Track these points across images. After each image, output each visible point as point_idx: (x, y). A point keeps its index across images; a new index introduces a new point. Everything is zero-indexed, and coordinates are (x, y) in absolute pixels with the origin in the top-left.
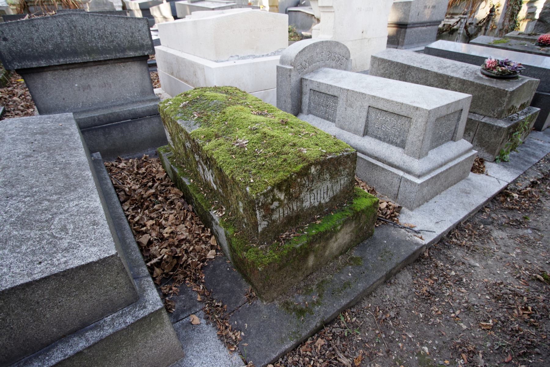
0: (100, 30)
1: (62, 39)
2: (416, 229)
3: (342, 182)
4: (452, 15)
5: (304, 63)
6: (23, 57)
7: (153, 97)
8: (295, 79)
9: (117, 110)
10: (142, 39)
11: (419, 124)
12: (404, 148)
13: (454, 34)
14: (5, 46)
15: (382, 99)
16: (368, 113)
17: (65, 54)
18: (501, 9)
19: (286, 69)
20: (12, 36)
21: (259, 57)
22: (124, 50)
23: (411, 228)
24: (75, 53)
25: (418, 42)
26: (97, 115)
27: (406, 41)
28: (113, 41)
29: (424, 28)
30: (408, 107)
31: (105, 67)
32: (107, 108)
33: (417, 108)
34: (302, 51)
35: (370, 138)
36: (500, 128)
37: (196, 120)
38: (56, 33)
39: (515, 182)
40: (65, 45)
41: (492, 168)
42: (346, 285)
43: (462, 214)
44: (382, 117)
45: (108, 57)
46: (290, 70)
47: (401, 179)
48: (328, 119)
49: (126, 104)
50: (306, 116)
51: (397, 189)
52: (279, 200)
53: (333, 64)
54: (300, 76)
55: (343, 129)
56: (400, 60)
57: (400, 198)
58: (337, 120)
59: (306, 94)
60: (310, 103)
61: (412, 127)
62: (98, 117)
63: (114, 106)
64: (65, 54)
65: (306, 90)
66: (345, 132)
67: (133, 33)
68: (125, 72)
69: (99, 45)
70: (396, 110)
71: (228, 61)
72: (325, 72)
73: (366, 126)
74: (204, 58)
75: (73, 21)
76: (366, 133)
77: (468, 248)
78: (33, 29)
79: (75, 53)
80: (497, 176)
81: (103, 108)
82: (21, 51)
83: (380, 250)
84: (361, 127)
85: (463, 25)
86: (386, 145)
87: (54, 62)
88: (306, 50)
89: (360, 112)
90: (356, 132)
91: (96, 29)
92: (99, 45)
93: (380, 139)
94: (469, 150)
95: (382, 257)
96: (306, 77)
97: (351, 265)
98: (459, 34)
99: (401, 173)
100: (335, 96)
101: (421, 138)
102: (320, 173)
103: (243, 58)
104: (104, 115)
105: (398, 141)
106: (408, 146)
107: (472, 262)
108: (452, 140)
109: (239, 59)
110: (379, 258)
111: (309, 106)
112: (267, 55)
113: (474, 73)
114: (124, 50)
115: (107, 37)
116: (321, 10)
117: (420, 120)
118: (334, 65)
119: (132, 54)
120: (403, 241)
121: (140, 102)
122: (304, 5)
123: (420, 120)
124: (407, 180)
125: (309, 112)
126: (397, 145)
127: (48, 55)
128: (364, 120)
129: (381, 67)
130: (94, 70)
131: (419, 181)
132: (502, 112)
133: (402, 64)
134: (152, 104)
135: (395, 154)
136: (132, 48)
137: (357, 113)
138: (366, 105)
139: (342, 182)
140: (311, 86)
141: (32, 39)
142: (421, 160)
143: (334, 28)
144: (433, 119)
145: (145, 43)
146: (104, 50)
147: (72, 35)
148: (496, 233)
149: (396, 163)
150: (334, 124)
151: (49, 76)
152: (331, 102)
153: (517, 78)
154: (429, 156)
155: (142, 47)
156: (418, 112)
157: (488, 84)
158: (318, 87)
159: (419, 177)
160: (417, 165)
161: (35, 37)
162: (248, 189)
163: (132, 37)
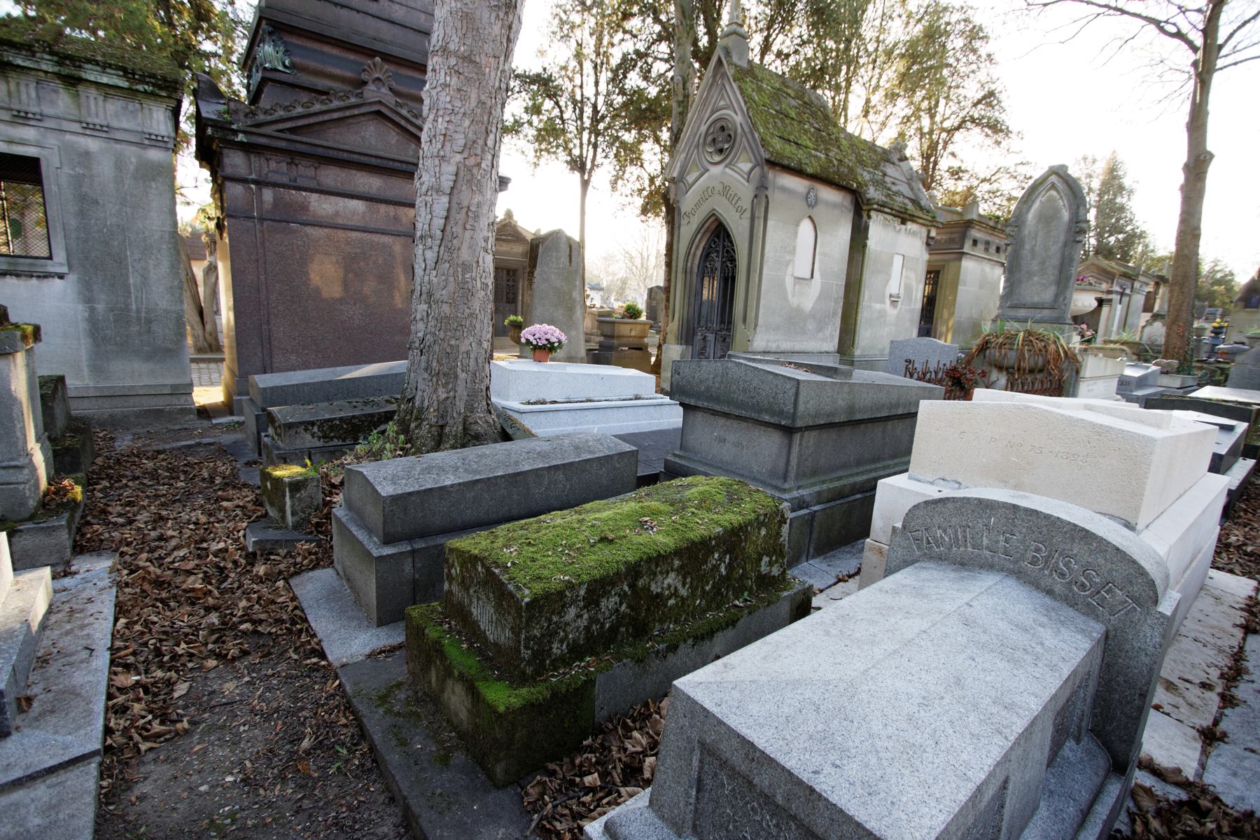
22: (760, 412)
42: (403, 743)
45: (744, 413)
64: (710, 398)
71: (932, 483)
79: (717, 400)
83: (456, 794)
87: (700, 404)
88: (950, 506)
95: (441, 794)
110: (439, 791)
119: (767, 418)
130: (735, 423)
146: (742, 405)
155: (781, 413)
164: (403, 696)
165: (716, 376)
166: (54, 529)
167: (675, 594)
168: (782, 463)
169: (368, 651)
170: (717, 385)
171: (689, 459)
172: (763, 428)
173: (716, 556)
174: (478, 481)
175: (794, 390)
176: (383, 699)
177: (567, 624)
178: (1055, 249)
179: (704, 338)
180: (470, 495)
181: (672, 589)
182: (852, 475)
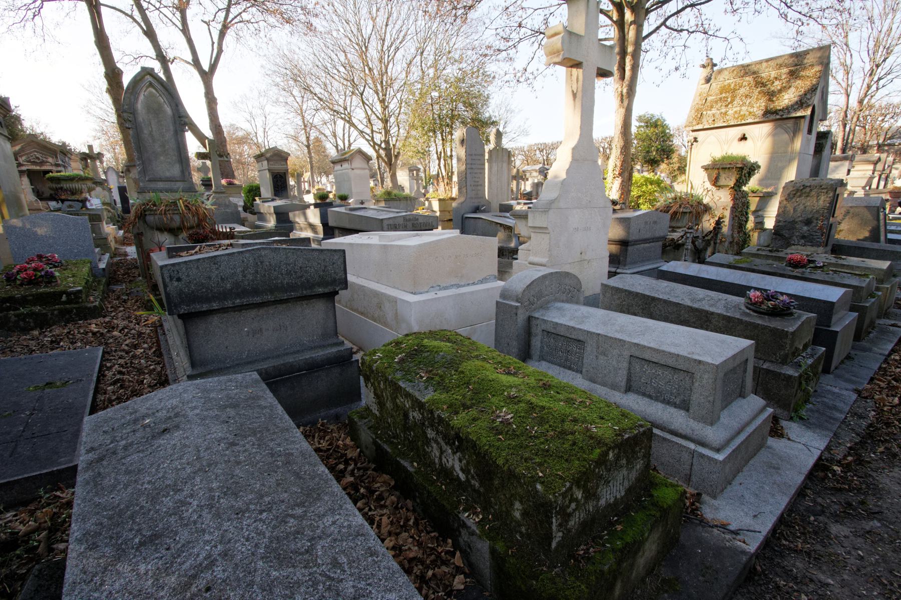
0: (289, 265)
1: (245, 276)
2: (732, 527)
3: (638, 467)
4: (673, 229)
5: (532, 298)
6: (193, 298)
7: (335, 341)
8: (522, 317)
9: (290, 359)
11: (704, 381)
12: (688, 410)
13: (681, 250)
14: (176, 287)
15: (649, 348)
16: (630, 363)
17: (244, 293)
18: (727, 220)
19: (511, 306)
20: (188, 276)
21: (464, 286)
22: (312, 286)
23: (724, 527)
24: (256, 292)
25: (643, 261)
26: (265, 367)
27: (628, 260)
28: (301, 277)
29: (647, 245)
30: (686, 359)
31: (284, 306)
32: (278, 356)
33: (700, 362)
34: (530, 285)
35: (636, 396)
36: (790, 377)
37: (426, 381)
39: (828, 448)
40: (246, 283)
41: (792, 428)
43: (783, 502)
44: (649, 370)
46: (517, 307)
47: (693, 453)
48: (570, 368)
50: (537, 363)
51: (688, 467)
52: (576, 500)
53: (564, 297)
54: (527, 314)
55: (594, 382)
56: (639, 289)
57: (694, 480)
58: (584, 370)
59: (536, 335)
60: (542, 347)
61: (697, 384)
62: (266, 369)
63: (287, 354)
65: (537, 330)
66: (598, 386)
67: (326, 267)
69: (285, 282)
70: (671, 362)
72: (559, 309)
73: (629, 380)
74: (394, 287)
75: (261, 256)
76: (628, 389)
77: (809, 554)
78: (214, 267)
79: (256, 292)
80: (803, 440)
81: (273, 358)
82: (193, 292)
84: (621, 379)
85: (690, 240)
86: (660, 406)
89: (618, 362)
90: (614, 387)
91: (286, 264)
93: (650, 397)
94: (762, 410)
95: (703, 576)
96: (536, 315)
97: (666, 591)
98: (687, 249)
99: (692, 446)
100: (579, 341)
101: (711, 399)
102: (618, 458)
103: (446, 288)
104: (274, 367)
105: (678, 401)
106: (694, 408)
107: (822, 577)
108: (740, 396)
109: (440, 289)
110: (701, 578)
111: (541, 351)
112: (474, 284)
113: (737, 307)
114: (312, 286)
115: (296, 272)
116: (531, 230)
117: (706, 376)
118: (565, 298)
119: (321, 290)
122: (484, 211)
123: (706, 376)
124: (702, 456)
125: (542, 358)
126: (675, 406)
127: (224, 296)
128: (625, 372)
129: (616, 297)
131: (720, 457)
132: (786, 356)
133: (644, 296)
134: (334, 350)
135: (676, 418)
137: (614, 363)
138: (626, 354)
139: (638, 467)
140: (544, 327)
141: (210, 278)
142: (715, 428)
143: (549, 250)
144: (721, 375)
147: (257, 272)
148: (835, 529)
149: (681, 431)
150: (579, 375)
151: (215, 320)
152: (574, 348)
153: (792, 314)
154: (722, 419)
156: (701, 367)
157: (760, 322)
158: (555, 328)
159: (718, 450)
160: (713, 434)
161: (213, 275)
162: (539, 487)
163: (324, 271)
172: (304, 302)
175: (342, 259)
178: (169, 135)
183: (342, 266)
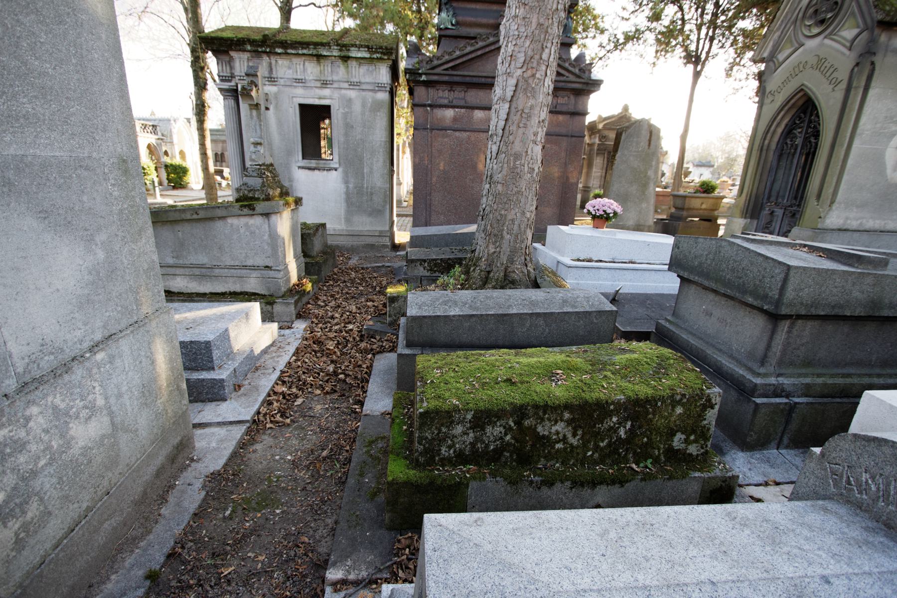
9: (710, 351)
10: (770, 288)
22: (745, 292)
28: (740, 278)
38: (706, 253)
42: (362, 475)
45: (729, 292)
49: (724, 353)
67: (764, 277)
68: (747, 320)
69: (728, 277)
83: (365, 520)
92: (728, 277)
119: (750, 300)
120: (351, 553)
121: (737, 361)
130: (723, 301)
136: (754, 294)
145: (770, 294)
155: (765, 297)
163: (760, 281)
164: (380, 445)
165: (709, 253)
166: (289, 304)
167: (564, 439)
168: (762, 347)
169: (383, 410)
170: (709, 262)
171: (677, 325)
173: (615, 419)
174: (473, 315)
175: (782, 276)
176: (371, 443)
177: (454, 436)
179: (772, 213)
180: (467, 324)
181: (561, 436)
182: (870, 375)
183: (780, 284)
